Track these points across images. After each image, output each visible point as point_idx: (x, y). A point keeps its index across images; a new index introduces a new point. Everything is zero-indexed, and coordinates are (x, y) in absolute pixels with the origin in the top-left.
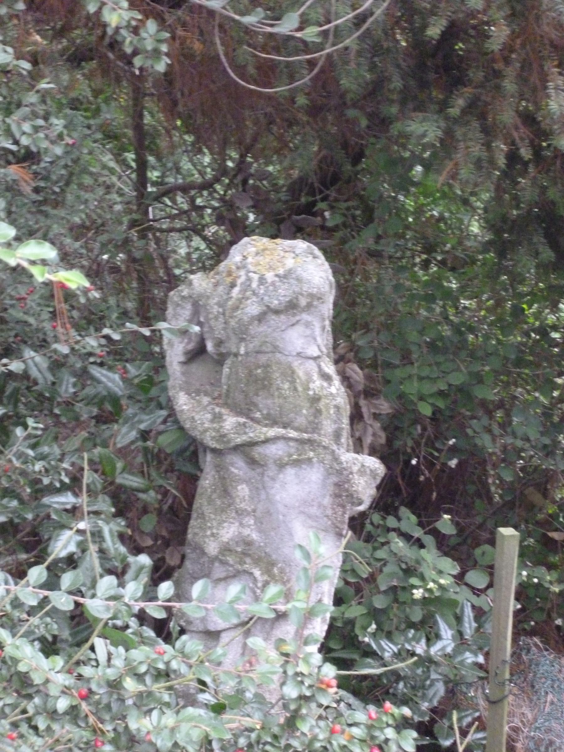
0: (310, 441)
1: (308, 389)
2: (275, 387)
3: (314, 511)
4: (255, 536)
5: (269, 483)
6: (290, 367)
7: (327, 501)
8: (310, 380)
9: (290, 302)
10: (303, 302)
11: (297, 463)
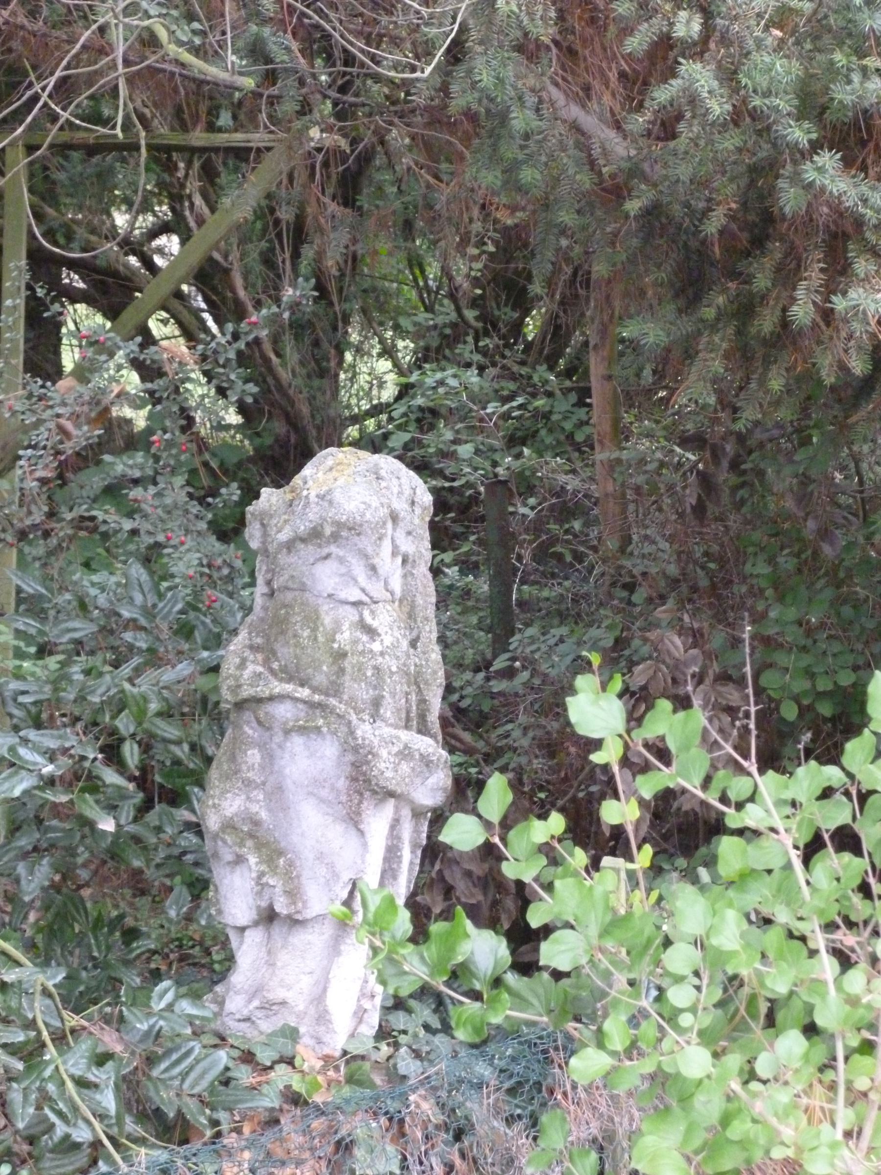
0: (320, 706)
1: (334, 641)
2: (290, 633)
3: (324, 793)
4: (264, 815)
5: (278, 752)
6: (316, 612)
7: (342, 783)
8: (337, 627)
9: (314, 528)
10: (328, 530)
11: (303, 730)
